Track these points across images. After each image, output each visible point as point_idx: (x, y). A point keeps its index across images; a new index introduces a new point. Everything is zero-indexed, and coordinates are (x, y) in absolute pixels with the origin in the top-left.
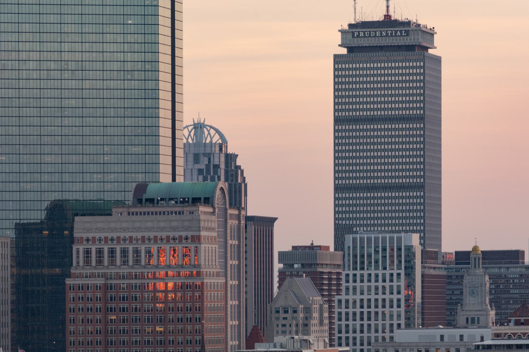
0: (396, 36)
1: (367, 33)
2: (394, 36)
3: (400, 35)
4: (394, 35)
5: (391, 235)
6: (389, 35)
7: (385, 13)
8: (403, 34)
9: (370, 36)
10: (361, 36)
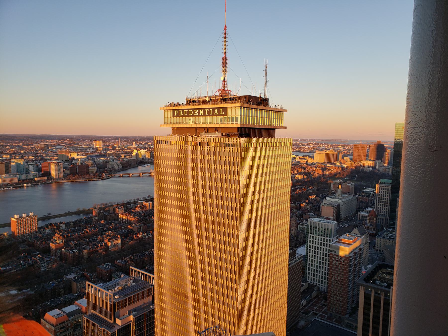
0: (213, 115)
1: (186, 111)
2: (211, 115)
4: (211, 114)
5: (386, 187)
6: (207, 114)
7: (221, 87)
8: (221, 114)
9: (188, 116)
10: (180, 115)
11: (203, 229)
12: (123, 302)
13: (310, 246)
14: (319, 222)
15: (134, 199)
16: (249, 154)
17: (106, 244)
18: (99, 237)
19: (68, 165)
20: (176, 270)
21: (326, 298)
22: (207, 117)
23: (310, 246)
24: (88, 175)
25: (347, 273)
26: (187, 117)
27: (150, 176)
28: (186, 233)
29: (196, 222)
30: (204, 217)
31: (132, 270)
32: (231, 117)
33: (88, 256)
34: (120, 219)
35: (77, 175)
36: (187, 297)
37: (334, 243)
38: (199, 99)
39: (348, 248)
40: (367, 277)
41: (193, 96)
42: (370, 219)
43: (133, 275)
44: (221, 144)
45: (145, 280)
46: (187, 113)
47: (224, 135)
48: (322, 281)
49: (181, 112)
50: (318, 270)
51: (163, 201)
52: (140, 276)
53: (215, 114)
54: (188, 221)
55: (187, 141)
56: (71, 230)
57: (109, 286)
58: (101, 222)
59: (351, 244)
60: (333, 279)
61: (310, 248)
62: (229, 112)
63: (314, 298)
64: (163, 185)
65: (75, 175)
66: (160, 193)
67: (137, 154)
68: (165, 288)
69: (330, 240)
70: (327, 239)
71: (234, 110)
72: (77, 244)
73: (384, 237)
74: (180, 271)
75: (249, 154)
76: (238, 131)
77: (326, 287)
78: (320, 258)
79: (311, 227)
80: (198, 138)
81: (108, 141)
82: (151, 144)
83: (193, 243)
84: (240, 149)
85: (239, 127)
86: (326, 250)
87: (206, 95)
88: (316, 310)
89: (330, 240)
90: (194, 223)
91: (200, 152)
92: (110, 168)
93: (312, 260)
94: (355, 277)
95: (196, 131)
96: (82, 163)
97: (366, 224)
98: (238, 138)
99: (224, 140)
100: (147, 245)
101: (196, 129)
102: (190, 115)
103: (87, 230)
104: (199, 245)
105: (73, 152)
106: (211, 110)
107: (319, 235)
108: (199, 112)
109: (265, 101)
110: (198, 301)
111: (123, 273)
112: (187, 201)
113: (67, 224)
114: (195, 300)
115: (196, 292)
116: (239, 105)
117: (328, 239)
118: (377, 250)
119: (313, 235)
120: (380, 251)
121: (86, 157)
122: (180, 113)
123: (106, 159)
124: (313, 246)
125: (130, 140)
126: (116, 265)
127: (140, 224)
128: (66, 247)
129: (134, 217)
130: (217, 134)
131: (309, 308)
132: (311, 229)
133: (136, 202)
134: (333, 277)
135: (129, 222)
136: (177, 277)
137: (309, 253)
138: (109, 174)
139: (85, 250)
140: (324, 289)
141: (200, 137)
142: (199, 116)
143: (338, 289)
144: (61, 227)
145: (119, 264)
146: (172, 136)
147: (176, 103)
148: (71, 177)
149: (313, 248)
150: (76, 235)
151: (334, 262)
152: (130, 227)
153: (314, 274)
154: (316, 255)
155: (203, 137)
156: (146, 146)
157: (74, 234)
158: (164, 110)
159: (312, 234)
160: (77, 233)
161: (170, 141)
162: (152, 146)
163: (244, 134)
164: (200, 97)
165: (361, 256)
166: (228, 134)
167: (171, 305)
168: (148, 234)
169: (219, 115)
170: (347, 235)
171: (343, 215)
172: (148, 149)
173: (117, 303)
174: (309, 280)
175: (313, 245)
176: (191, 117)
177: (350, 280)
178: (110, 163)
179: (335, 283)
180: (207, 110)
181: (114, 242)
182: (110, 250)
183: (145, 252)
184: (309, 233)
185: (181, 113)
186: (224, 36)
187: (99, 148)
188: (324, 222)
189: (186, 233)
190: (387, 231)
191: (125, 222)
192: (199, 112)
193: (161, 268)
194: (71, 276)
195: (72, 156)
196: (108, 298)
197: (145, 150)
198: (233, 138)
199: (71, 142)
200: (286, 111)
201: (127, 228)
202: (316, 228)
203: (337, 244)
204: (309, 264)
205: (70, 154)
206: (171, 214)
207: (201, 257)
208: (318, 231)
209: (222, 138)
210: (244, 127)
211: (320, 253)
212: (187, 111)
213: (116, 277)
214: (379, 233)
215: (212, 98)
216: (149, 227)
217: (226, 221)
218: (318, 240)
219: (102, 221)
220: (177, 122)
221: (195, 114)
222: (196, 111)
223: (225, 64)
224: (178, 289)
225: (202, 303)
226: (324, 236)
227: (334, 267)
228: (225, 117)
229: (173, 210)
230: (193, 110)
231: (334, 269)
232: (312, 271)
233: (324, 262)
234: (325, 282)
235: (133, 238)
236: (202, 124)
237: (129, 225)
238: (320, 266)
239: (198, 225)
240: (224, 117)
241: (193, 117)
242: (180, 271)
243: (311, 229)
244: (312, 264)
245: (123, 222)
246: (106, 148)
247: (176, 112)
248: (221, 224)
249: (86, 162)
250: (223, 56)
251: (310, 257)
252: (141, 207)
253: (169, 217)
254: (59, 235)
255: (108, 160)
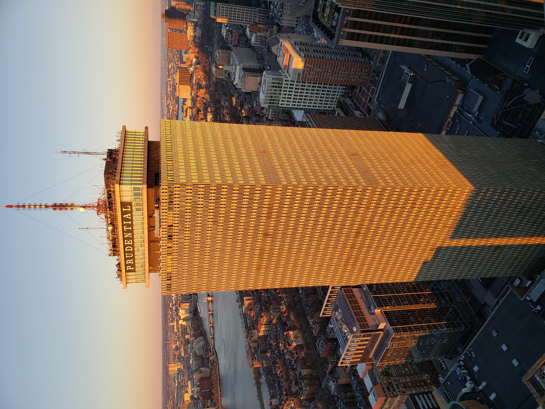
0: (132, 220)
1: (128, 255)
2: (132, 222)
3: (130, 215)
4: (130, 223)
5: (221, 10)
6: (130, 228)
7: (94, 212)
8: (129, 210)
9: (133, 252)
10: (132, 263)
11: (276, 229)
12: (360, 322)
13: (293, 105)
14: (265, 93)
15: (241, 319)
16: (182, 173)
17: (295, 348)
18: (287, 357)
19: (200, 403)
20: (323, 260)
21: (353, 88)
22: (134, 228)
23: (293, 105)
24: (212, 378)
25: (324, 61)
26: (135, 254)
27: (212, 301)
28: (281, 249)
29: (269, 238)
30: (262, 228)
31: (324, 314)
32: (133, 197)
33: (309, 368)
34: (265, 334)
35: (212, 390)
36: (353, 247)
37: (290, 76)
38: (111, 239)
39: (295, 59)
40: (328, 35)
41: (107, 247)
42: (259, 31)
43: (330, 313)
44: (170, 209)
45: (335, 297)
46: (130, 254)
47: (157, 205)
48: (333, 92)
49: (128, 262)
50: (320, 95)
51: (243, 279)
52: (330, 303)
53: (130, 218)
54: (267, 248)
55: (166, 253)
56: (278, 392)
57: (343, 340)
58: (269, 356)
59: (290, 55)
60: (331, 78)
61: (295, 105)
62: (126, 199)
63: (352, 101)
64: (224, 280)
65: (213, 393)
66: (233, 283)
67: (184, 320)
68: (344, 272)
69: (286, 81)
70: (285, 84)
71: (124, 194)
72: (295, 383)
73: (281, 16)
74: (324, 255)
75: (182, 173)
76: (152, 187)
77: (340, 87)
78: (306, 93)
79: (270, 103)
80: (163, 238)
81: (169, 356)
82: (171, 303)
83: (292, 241)
84: (176, 184)
85: (146, 186)
86: (297, 85)
87: (105, 230)
88: (366, 99)
89: (286, 81)
90: (269, 240)
91: (181, 236)
92: (203, 351)
93: (309, 103)
94: (328, 52)
95: (153, 241)
96: (198, 386)
97: (265, 37)
98: (162, 187)
99: (164, 205)
100: (295, 299)
101: (150, 241)
102: (132, 250)
103: (279, 372)
104: (294, 233)
105: (184, 399)
107: (280, 94)
108: (128, 239)
109: (111, 153)
110: (358, 233)
111: (327, 325)
112: (243, 250)
113: (272, 397)
114: (356, 237)
115: (348, 236)
116: (117, 186)
117: (284, 82)
118: (296, 25)
119: (281, 101)
120: (297, 21)
121: (189, 382)
122: (130, 263)
123: (191, 357)
124: (293, 102)
125: (166, 330)
126: (318, 335)
127: (271, 309)
128: (299, 395)
129: (262, 317)
130: (156, 215)
131: (363, 107)
132: (273, 103)
133: (245, 316)
134: (328, 78)
135: (269, 322)
136: (331, 259)
137: (301, 107)
138: (210, 351)
139: (302, 372)
140: (342, 89)
141: (161, 236)
142: (133, 239)
143: (342, 72)
144: (276, 404)
145: (318, 330)
146: (161, 272)
147: (117, 268)
148: (215, 397)
149: (295, 102)
150: (285, 385)
151: (311, 76)
152: (274, 322)
153: (325, 101)
154: (303, 98)
155: (160, 232)
156: (174, 309)
157: (283, 387)
158: (127, 283)
159: (278, 102)
160: (282, 383)
161: (167, 274)
162: (174, 302)
163: (156, 180)
164: (109, 238)
165: (304, 44)
166: (156, 200)
167: (362, 264)
168: (282, 299)
169: (131, 212)
170: (279, 60)
171: (256, 65)
172: (177, 307)
173: (361, 329)
174: (333, 108)
175: (291, 102)
176: (135, 248)
177: (331, 58)
178: (197, 352)
179: (335, 75)
180: (125, 228)
181: (293, 339)
182: (301, 343)
183: (303, 301)
184: (278, 105)
185: (130, 262)
186: (21, 209)
187: (178, 367)
188: (264, 88)
189: (281, 249)
190: (273, 12)
191: (268, 327)
192: (128, 239)
193: (321, 278)
194: (332, 385)
195: (189, 399)
196: (356, 340)
197: (179, 310)
198: (162, 194)
199: (170, 402)
200: (124, 127)
201: (275, 325)
202: (272, 97)
203: (291, 71)
204: (313, 106)
205: (186, 401)
206: (259, 268)
207: (309, 231)
208: (275, 95)
209: (162, 208)
210: (146, 180)
211: (300, 93)
212: (126, 254)
213: (332, 333)
214: (276, 21)
215: (109, 222)
216: (274, 298)
217: (267, 202)
218: (286, 95)
219: (267, 356)
220: (142, 267)
221: (131, 243)
222: (127, 242)
223: (62, 207)
224: (345, 257)
225: (360, 228)
226: (281, 87)
227: (317, 76)
228: (133, 205)
229: (254, 267)
230: (125, 246)
231: (319, 77)
232: (322, 104)
233: (311, 88)
234: (335, 88)
235: (286, 316)
236: (143, 234)
237: (272, 322)
238: (317, 94)
239: (271, 235)
240: (134, 206)
241: (135, 246)
242: (324, 255)
243: (273, 103)
244: (314, 103)
245: (269, 330)
246: (178, 359)
247: (129, 268)
248: (270, 208)
249: (196, 381)
250: (50, 210)
251: (305, 106)
252: (251, 310)
253: (263, 271)
254: (285, 404)
255: (193, 354)
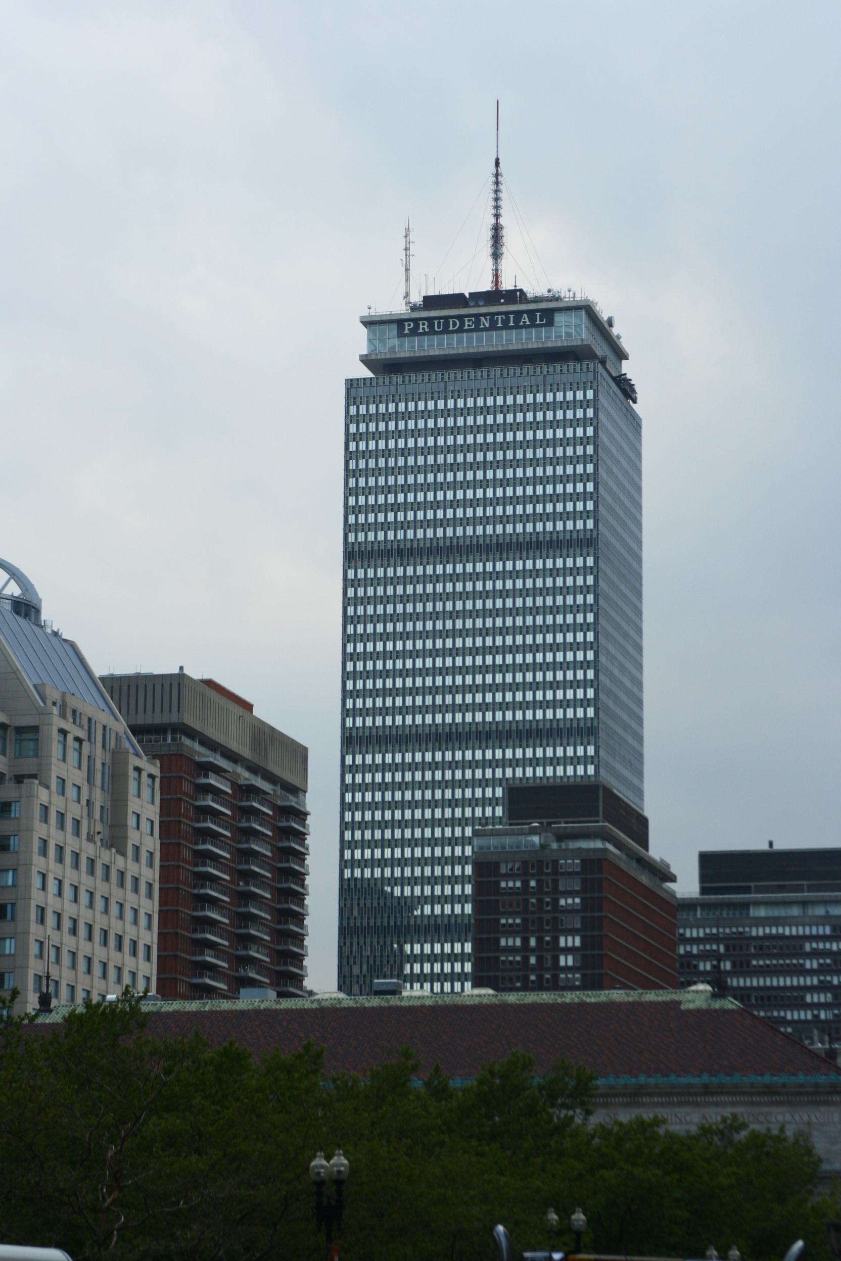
2: (512, 328)
3: (528, 323)
4: (512, 324)
6: (500, 325)
8: (538, 322)
10: (421, 331)
22: (499, 332)
102: (451, 328)
106: (512, 316)
122: (421, 327)
180: (500, 317)
185: (424, 327)
192: (478, 322)
212: (442, 321)
221: (466, 327)
247: (409, 325)
250: (493, 221)
